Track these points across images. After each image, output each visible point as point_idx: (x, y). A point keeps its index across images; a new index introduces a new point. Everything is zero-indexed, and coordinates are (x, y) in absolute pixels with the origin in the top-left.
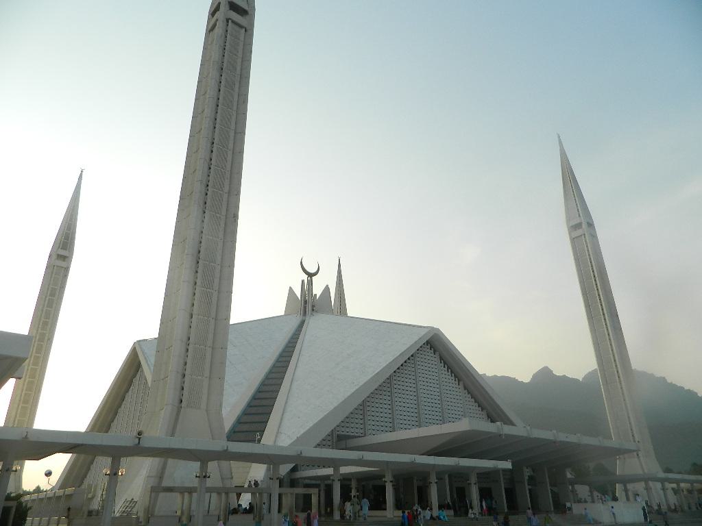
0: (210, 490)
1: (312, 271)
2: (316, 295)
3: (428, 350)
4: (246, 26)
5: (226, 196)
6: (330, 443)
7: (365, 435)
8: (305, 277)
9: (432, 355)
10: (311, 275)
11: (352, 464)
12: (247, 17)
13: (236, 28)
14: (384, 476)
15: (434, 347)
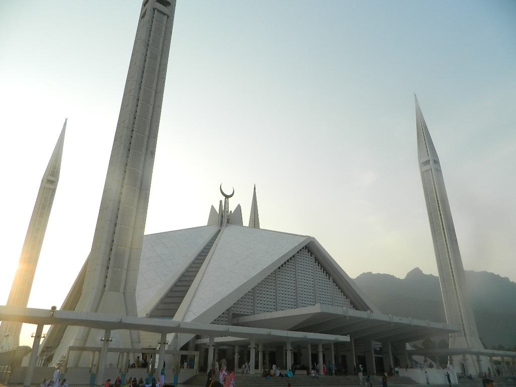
0: (111, 350)
1: (229, 194)
2: (231, 211)
3: (307, 253)
4: (167, 13)
5: (146, 139)
6: (226, 319)
7: (254, 314)
8: (223, 198)
9: (309, 257)
10: (227, 197)
11: (230, 336)
12: (169, 7)
13: (162, 16)
14: (250, 345)
15: (310, 250)
